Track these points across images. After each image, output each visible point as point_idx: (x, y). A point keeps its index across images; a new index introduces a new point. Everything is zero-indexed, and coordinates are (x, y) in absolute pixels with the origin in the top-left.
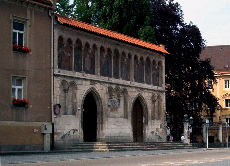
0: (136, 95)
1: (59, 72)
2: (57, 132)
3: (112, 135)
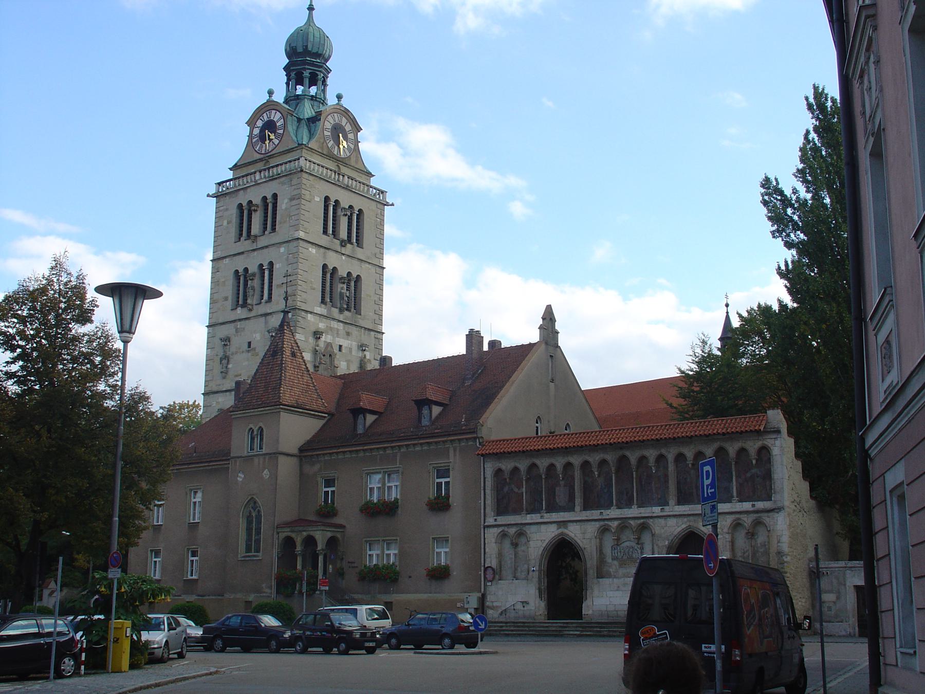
0: (679, 529)
1: (496, 520)
2: (493, 606)
3: (611, 608)
